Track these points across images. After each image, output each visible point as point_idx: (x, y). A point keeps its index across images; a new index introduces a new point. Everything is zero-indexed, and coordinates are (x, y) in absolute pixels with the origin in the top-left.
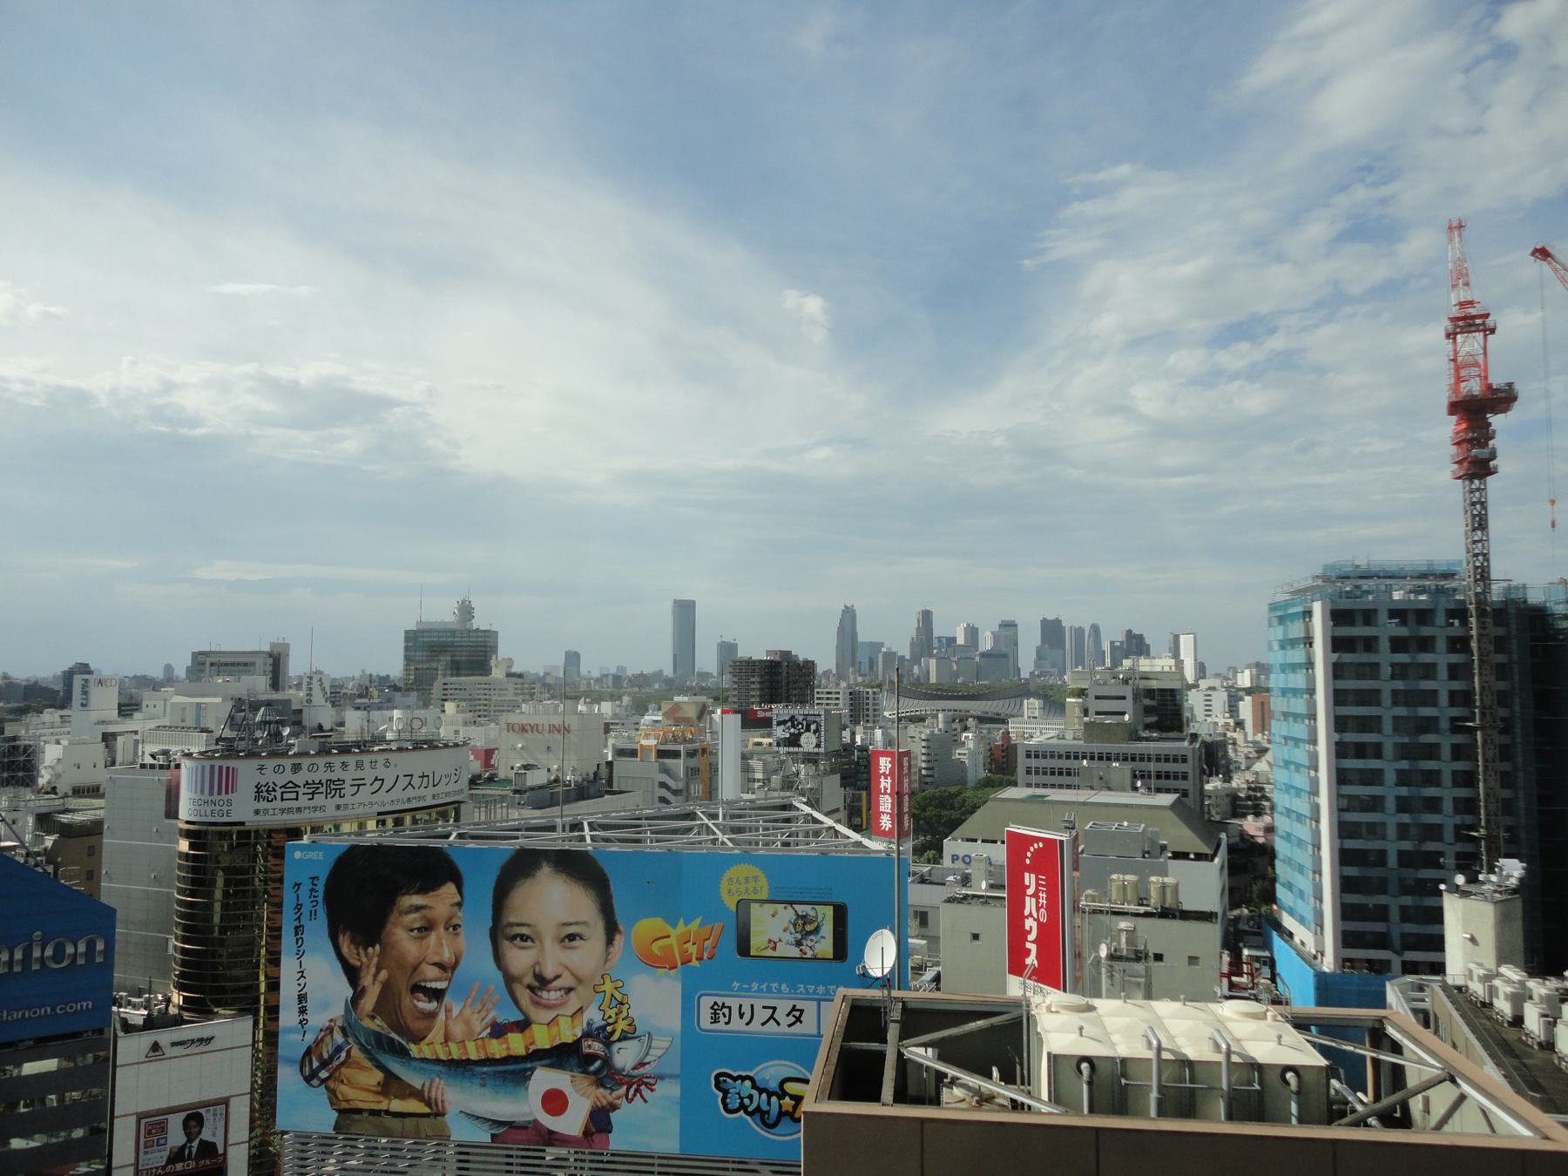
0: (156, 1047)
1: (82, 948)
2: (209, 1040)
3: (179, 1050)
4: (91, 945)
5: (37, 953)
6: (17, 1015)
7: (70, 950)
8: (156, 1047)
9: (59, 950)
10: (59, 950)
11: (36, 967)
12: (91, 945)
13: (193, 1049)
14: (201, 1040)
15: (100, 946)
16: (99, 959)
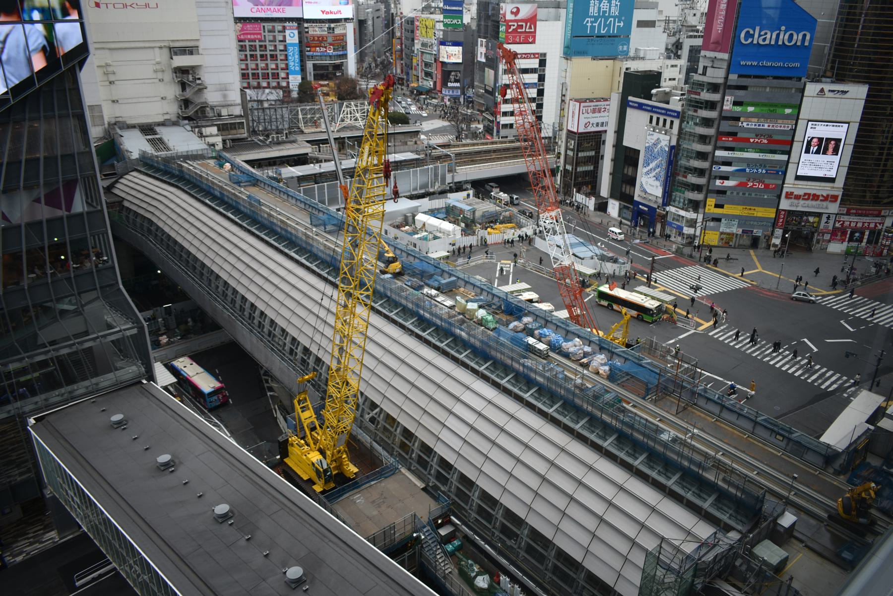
0: (822, 90)
1: (800, 37)
2: (846, 92)
3: (831, 95)
4: (805, 36)
5: (781, 37)
6: (769, 64)
7: (795, 37)
8: (822, 90)
9: (791, 36)
10: (791, 36)
11: (780, 43)
12: (805, 36)
13: (837, 96)
14: (843, 92)
15: (808, 37)
16: (806, 44)
